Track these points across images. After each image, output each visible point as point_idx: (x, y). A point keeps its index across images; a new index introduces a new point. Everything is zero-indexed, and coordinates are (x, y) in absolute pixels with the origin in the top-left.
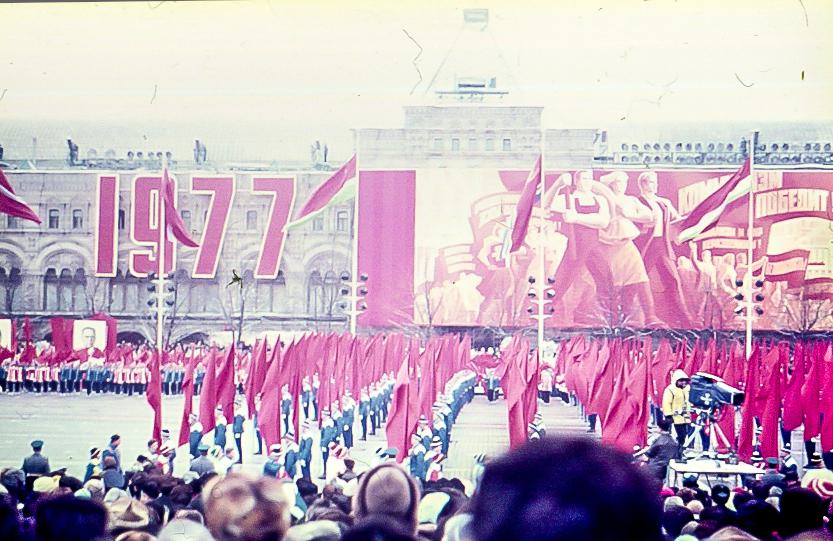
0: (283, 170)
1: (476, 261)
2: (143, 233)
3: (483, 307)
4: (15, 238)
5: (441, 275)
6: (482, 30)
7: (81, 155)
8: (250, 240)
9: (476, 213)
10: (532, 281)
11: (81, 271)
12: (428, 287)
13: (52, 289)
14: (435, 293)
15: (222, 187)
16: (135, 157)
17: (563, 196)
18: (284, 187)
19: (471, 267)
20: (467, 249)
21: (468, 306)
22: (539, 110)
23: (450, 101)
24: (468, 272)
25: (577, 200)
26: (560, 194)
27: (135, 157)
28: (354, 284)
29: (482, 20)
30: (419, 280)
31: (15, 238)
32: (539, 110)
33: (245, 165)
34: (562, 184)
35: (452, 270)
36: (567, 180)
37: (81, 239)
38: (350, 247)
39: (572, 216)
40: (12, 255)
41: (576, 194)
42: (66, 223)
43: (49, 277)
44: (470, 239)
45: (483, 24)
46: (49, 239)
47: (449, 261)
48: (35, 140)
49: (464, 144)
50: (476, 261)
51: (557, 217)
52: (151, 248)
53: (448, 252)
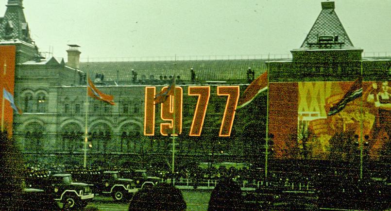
0: (233, 84)
1: (330, 129)
2: (167, 114)
3: (332, 150)
4: (108, 118)
5: (310, 133)
6: (331, 13)
7: (139, 77)
8: (217, 118)
9: (329, 102)
10: (357, 137)
11: (138, 134)
12: (305, 140)
13: (124, 141)
14: (308, 143)
15: (204, 92)
16: (163, 79)
17: (373, 95)
18: (233, 92)
19: (326, 130)
20: (324, 121)
21: (324, 150)
22: (362, 51)
23: (316, 49)
24: (324, 133)
25: (380, 97)
26: (371, 94)
27: (163, 79)
28: (267, 139)
29: (330, 8)
30: (300, 137)
31: (108, 118)
32: (362, 51)
33: (215, 82)
34: (372, 88)
35: (316, 132)
36: (375, 86)
37: (138, 118)
38: (265, 121)
39: (378, 104)
40: (105, 125)
41: (380, 93)
42: (131, 108)
43: (124, 135)
44: (326, 117)
45: (331, 10)
46: (123, 118)
47: (314, 127)
48: (118, 72)
49: (322, 69)
50: (330, 129)
51: (370, 105)
52: (170, 122)
53: (314, 123)
